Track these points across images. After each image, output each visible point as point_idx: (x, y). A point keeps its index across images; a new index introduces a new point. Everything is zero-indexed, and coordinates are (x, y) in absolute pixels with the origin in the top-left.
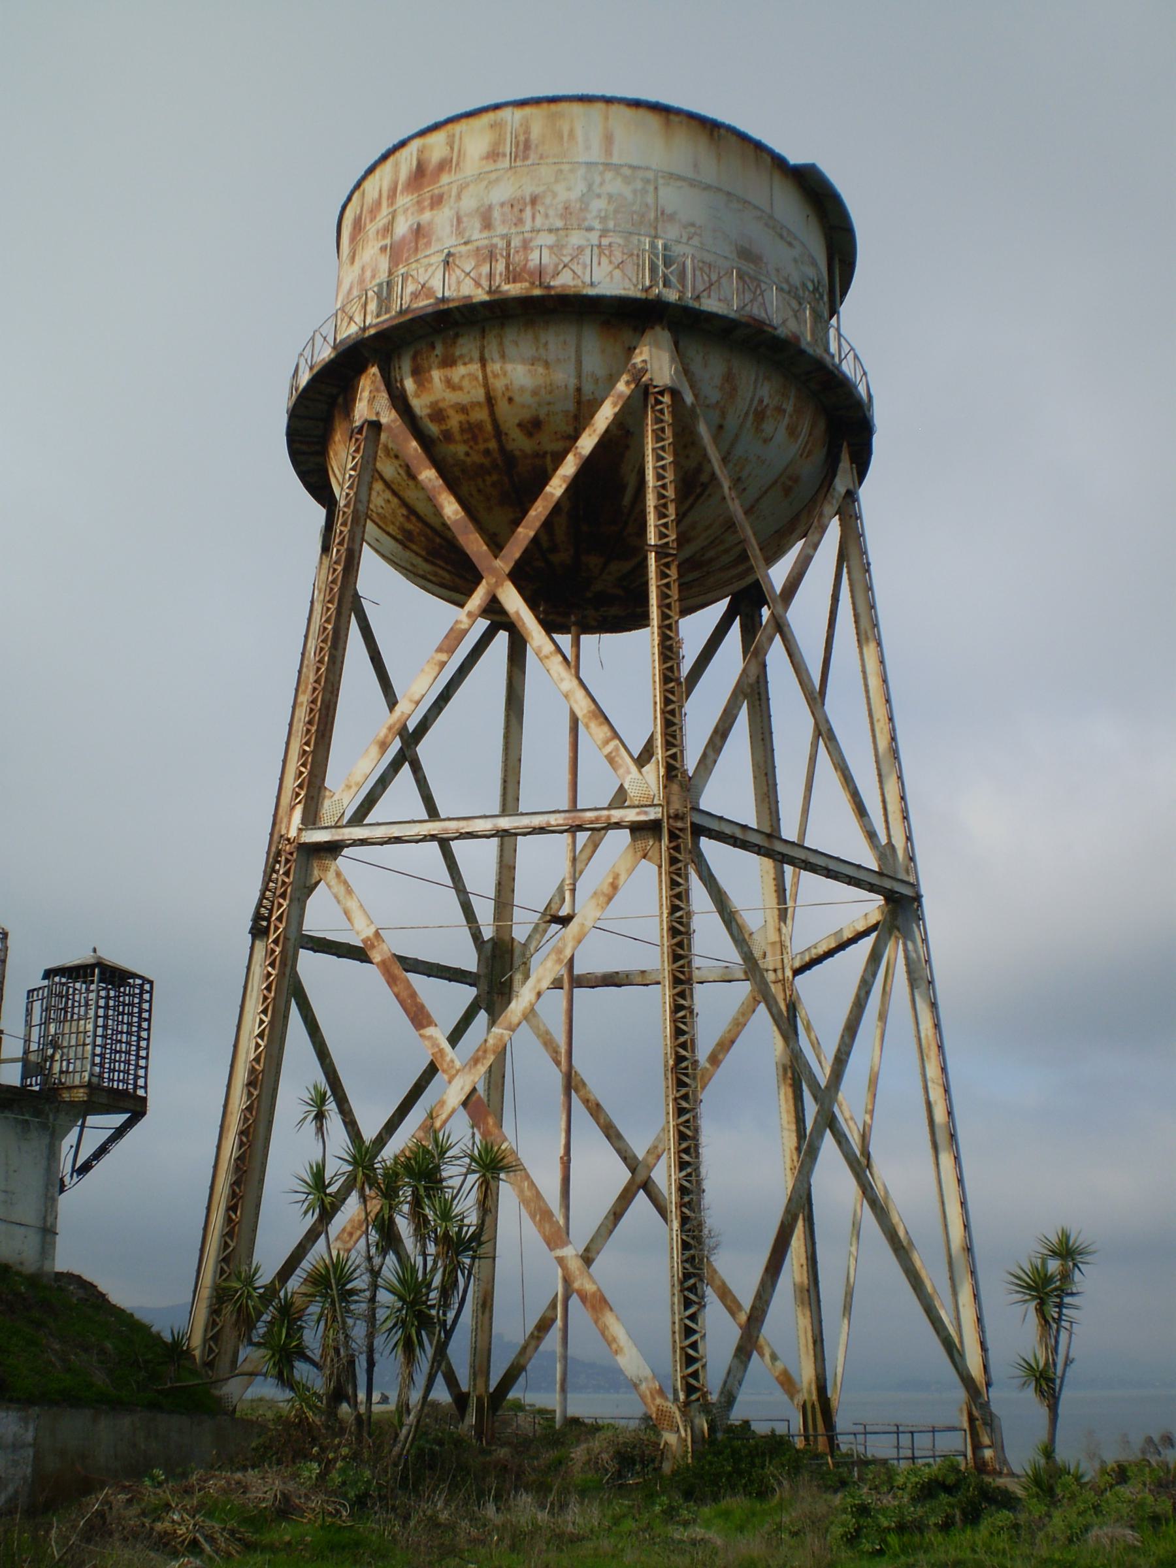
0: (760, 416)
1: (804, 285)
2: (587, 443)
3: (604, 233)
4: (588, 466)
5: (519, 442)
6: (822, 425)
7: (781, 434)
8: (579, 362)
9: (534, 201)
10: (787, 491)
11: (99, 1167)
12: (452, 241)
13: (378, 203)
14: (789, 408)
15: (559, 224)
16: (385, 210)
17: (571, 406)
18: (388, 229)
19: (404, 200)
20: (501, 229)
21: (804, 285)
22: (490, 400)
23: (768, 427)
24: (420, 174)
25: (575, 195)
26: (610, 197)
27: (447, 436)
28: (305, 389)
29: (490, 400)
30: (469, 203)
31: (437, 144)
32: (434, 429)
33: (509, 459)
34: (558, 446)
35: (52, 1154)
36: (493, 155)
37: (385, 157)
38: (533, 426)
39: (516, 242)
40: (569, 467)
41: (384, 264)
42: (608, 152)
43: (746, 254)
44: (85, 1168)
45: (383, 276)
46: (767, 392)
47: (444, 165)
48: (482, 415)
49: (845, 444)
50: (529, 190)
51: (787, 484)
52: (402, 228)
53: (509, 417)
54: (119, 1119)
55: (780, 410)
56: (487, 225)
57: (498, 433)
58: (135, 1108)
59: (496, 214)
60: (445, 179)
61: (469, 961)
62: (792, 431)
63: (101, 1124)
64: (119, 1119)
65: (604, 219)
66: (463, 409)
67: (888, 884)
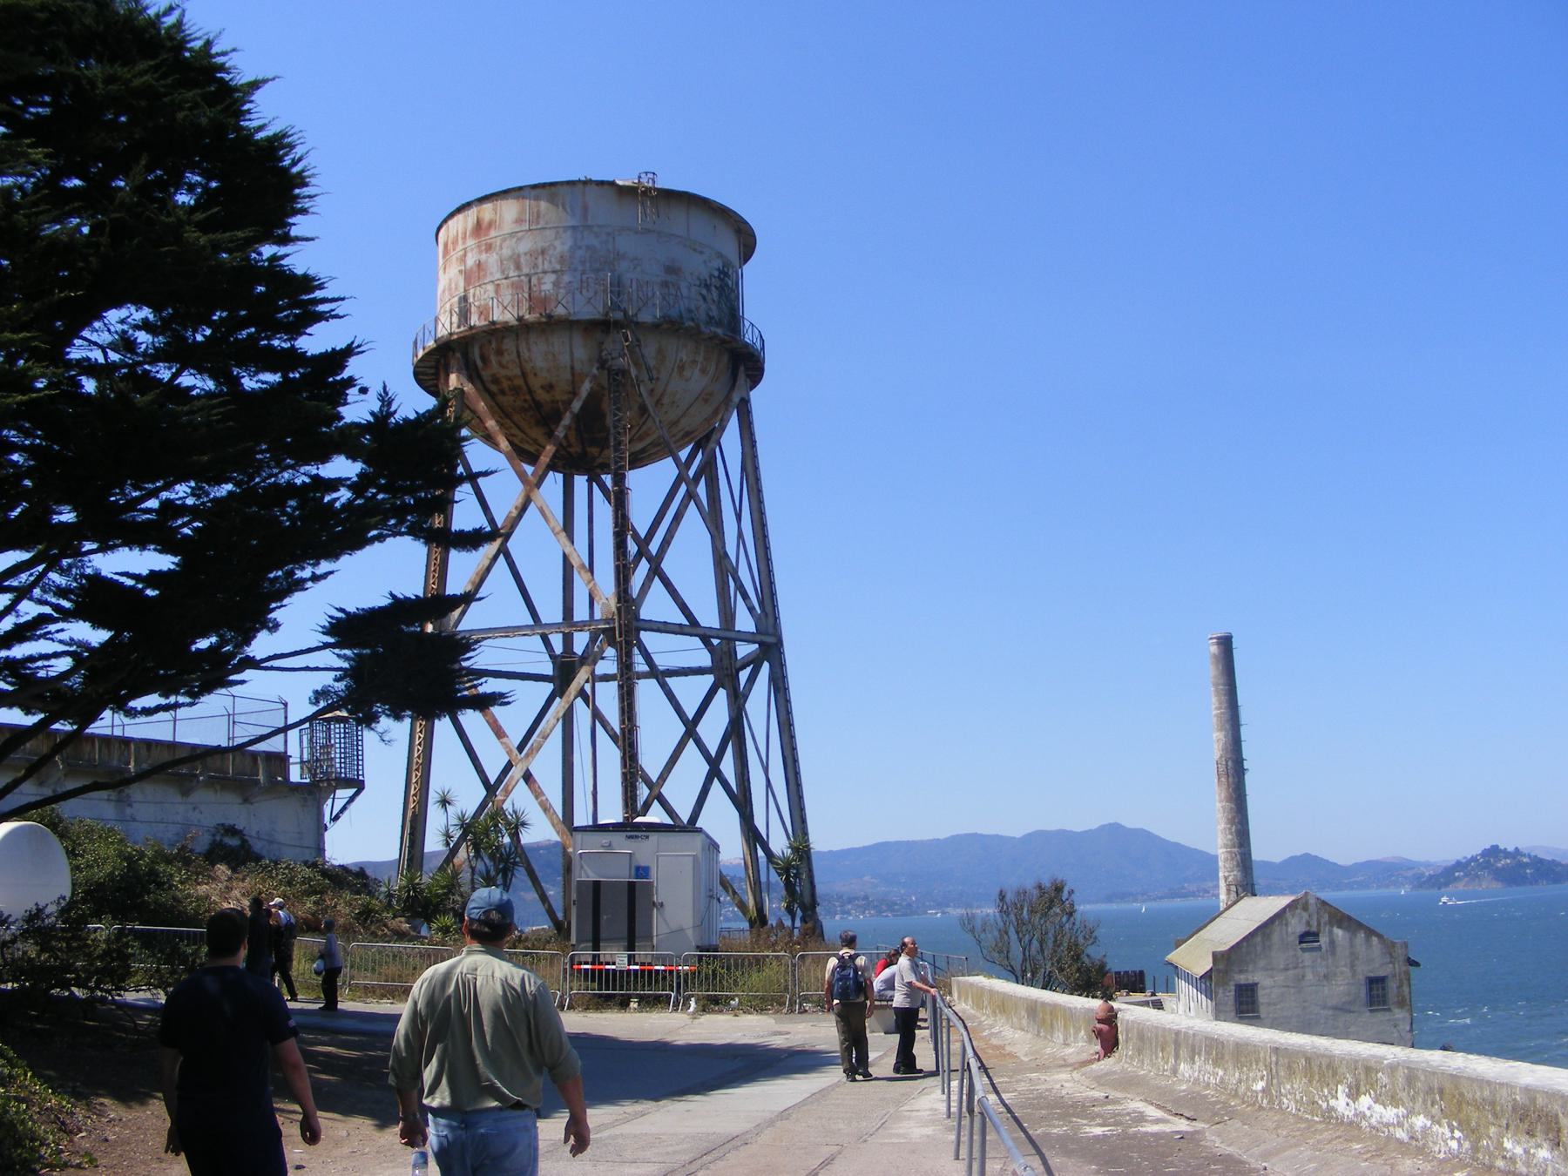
0: (682, 368)
1: (711, 276)
2: (576, 406)
3: (583, 273)
4: (577, 418)
5: (542, 396)
6: (725, 358)
7: (697, 372)
8: (572, 353)
9: (543, 252)
10: (706, 401)
11: (344, 817)
12: (499, 276)
13: (455, 242)
14: (700, 359)
15: (558, 267)
16: (460, 247)
17: (569, 376)
18: (463, 259)
19: (471, 242)
20: (526, 270)
21: (711, 276)
22: (524, 375)
23: (687, 373)
24: (479, 228)
25: (566, 247)
26: (588, 247)
27: (503, 392)
28: (421, 360)
29: (524, 375)
30: (506, 252)
31: (487, 210)
32: (494, 388)
33: (538, 405)
34: (565, 397)
35: (320, 814)
36: (519, 221)
37: (459, 210)
38: (549, 387)
39: (534, 280)
40: (567, 420)
41: (462, 284)
42: (585, 217)
43: (672, 270)
44: (335, 819)
45: (461, 292)
46: (684, 355)
47: (491, 224)
48: (519, 382)
49: (742, 368)
50: (541, 244)
51: (705, 397)
52: (470, 261)
53: (535, 383)
54: (351, 791)
55: (694, 362)
56: (518, 267)
57: (530, 391)
58: (359, 786)
59: (522, 260)
60: (493, 233)
61: (547, 668)
62: (703, 371)
63: (344, 794)
64: (351, 791)
65: (583, 263)
66: (509, 379)
67: (759, 638)
